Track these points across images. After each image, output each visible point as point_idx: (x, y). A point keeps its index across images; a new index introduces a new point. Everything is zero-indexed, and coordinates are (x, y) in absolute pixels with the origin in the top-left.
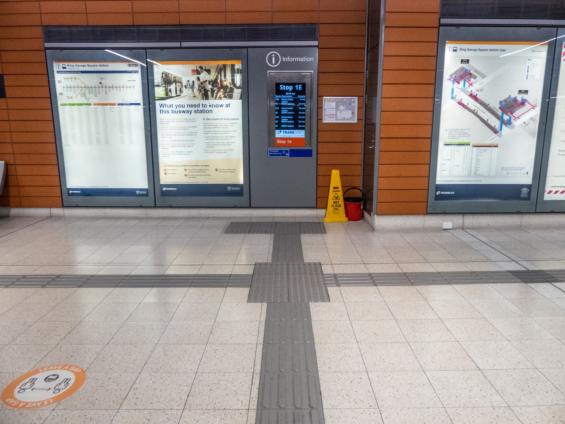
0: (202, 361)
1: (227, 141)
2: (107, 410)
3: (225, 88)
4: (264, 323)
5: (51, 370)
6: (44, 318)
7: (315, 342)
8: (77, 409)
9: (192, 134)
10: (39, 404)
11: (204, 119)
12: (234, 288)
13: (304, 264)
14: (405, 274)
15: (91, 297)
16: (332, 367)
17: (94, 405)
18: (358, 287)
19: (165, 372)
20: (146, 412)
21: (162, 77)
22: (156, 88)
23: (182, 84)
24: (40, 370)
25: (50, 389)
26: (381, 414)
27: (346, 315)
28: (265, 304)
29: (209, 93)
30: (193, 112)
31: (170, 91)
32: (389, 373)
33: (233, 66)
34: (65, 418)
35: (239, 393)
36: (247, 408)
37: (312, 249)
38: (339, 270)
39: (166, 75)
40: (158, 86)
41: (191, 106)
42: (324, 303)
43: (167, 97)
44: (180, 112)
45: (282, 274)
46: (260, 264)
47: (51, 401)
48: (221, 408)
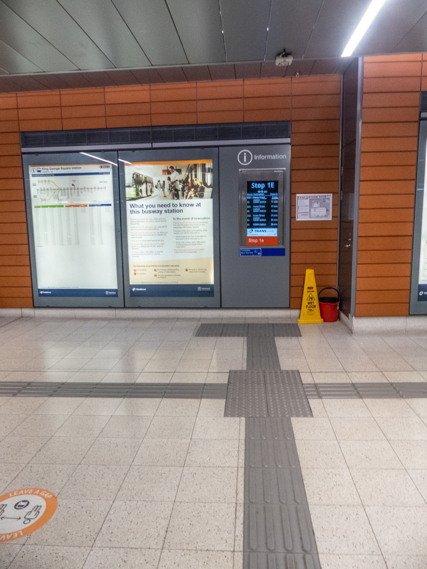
0: (180, 486)
1: (198, 240)
2: (80, 547)
3: (196, 187)
4: (244, 441)
5: (21, 494)
6: (15, 432)
7: (301, 466)
8: (49, 545)
9: (162, 234)
10: (8, 537)
11: (174, 219)
12: (210, 400)
13: (282, 372)
14: (392, 384)
15: (62, 407)
16: (323, 499)
17: (66, 540)
18: (342, 400)
19: (140, 501)
20: (121, 551)
21: (133, 177)
22: (127, 189)
23: (152, 184)
24: (11, 495)
25: (20, 518)
26: (386, 563)
27: (332, 433)
28: (243, 419)
29: (180, 193)
30: (163, 212)
31: (141, 191)
32: (389, 508)
33: (204, 165)
34: (35, 555)
35: (222, 529)
36: (232, 550)
37: (291, 354)
38: (320, 379)
39: (137, 176)
40: (129, 186)
41: (161, 206)
42: (306, 419)
43: (138, 197)
44: (150, 212)
45: (258, 384)
46: (235, 372)
47: (22, 534)
48: (203, 548)
